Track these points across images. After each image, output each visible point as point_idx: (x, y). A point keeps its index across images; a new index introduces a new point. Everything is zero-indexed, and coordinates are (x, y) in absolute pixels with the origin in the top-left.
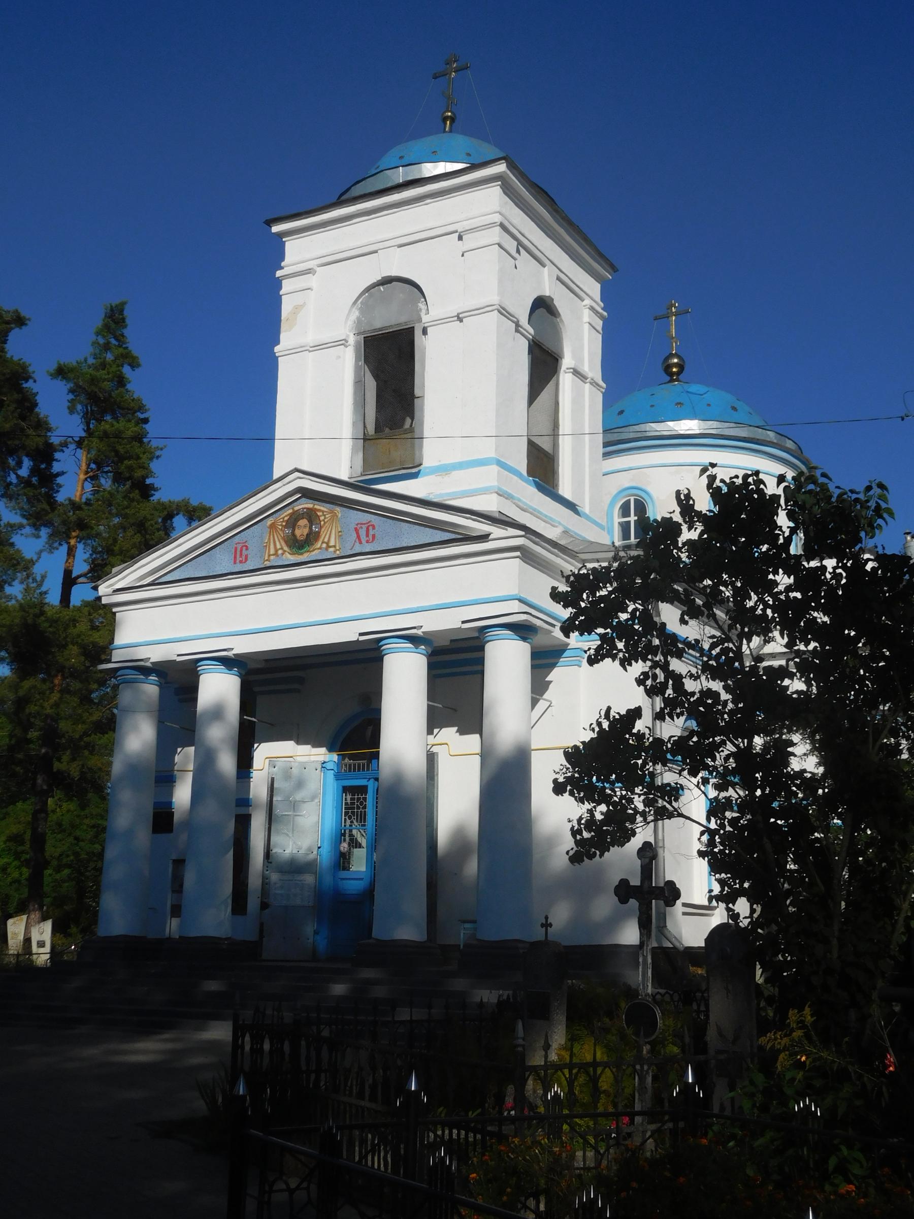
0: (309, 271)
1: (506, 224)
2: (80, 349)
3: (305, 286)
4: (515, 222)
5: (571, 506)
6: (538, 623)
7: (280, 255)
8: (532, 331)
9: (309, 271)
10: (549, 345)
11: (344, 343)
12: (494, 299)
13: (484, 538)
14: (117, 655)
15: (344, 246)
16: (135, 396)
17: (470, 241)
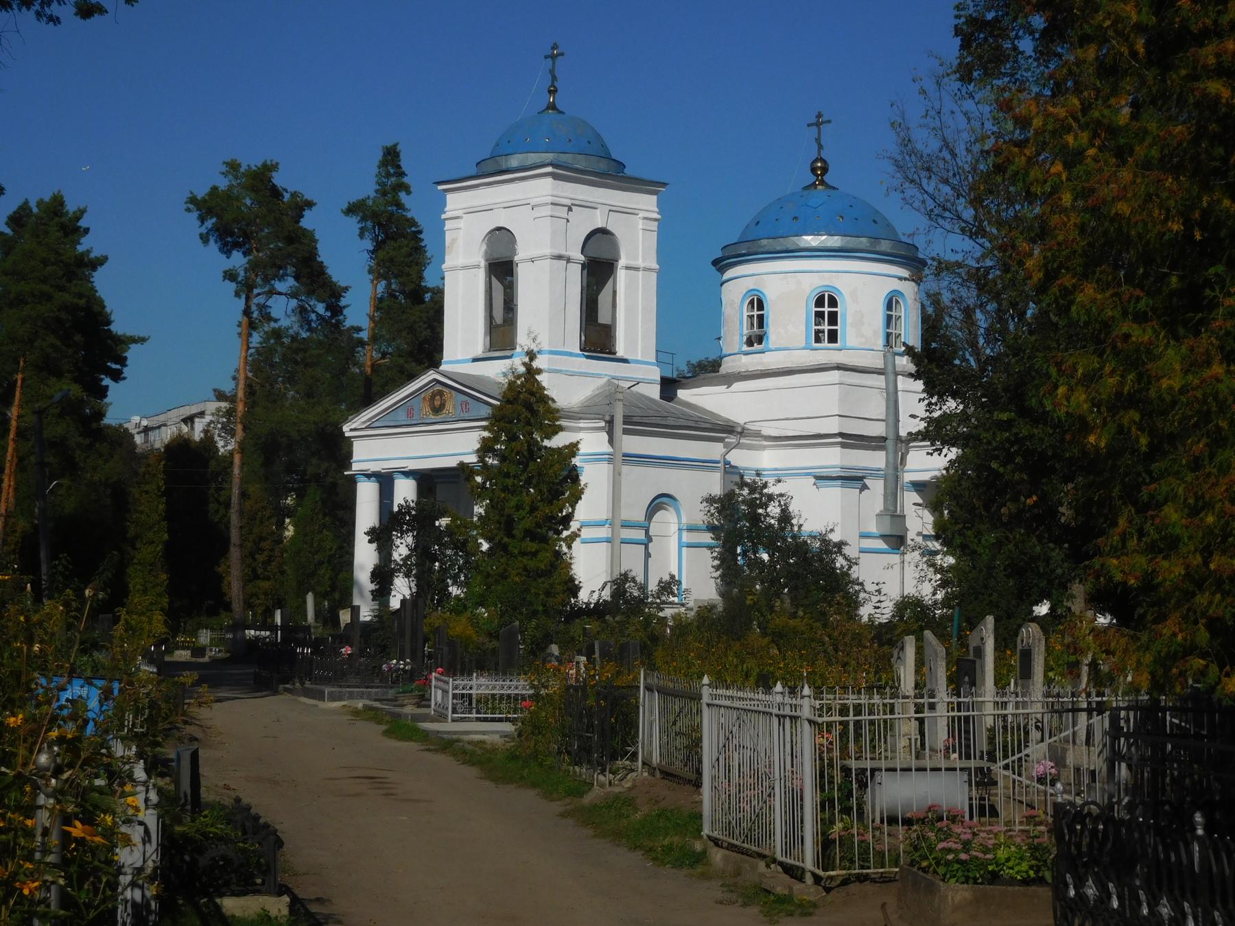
2: (366, 187)
3: (456, 226)
7: (444, 203)
8: (583, 258)
10: (605, 255)
11: (478, 267)
12: (548, 251)
14: (356, 467)
16: (409, 215)
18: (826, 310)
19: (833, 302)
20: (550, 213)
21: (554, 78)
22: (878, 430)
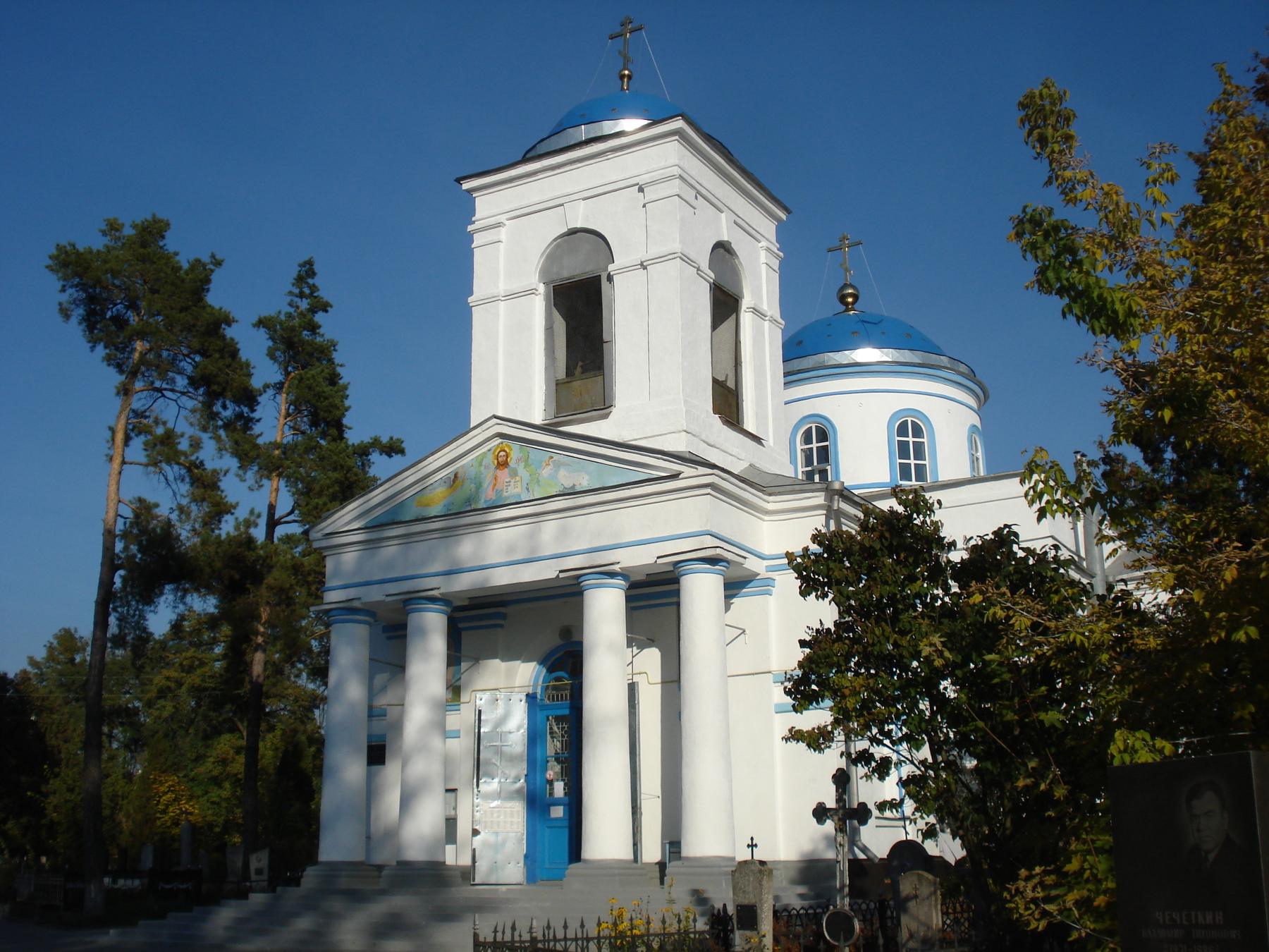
1: (685, 176)
4: (693, 173)
5: (757, 439)
6: (729, 556)
8: (712, 275)
10: (728, 287)
13: (675, 476)
17: (651, 193)
19: (918, 432)
20: (676, 191)
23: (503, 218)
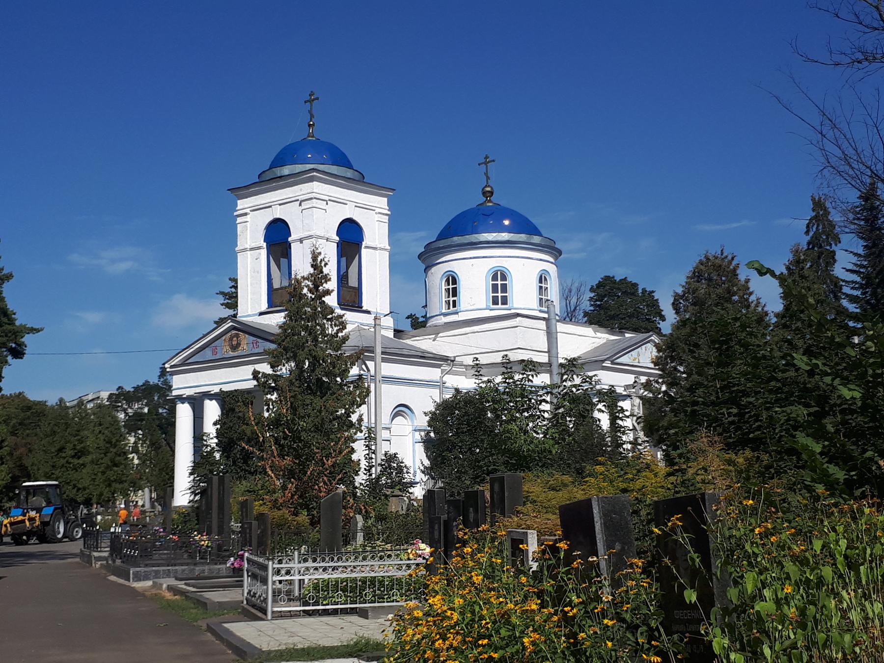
0: (246, 214)
8: (338, 238)
9: (246, 214)
15: (259, 203)
17: (305, 205)
18: (499, 283)
19: (504, 278)
21: (312, 116)
22: (543, 358)
23: (248, 211)
